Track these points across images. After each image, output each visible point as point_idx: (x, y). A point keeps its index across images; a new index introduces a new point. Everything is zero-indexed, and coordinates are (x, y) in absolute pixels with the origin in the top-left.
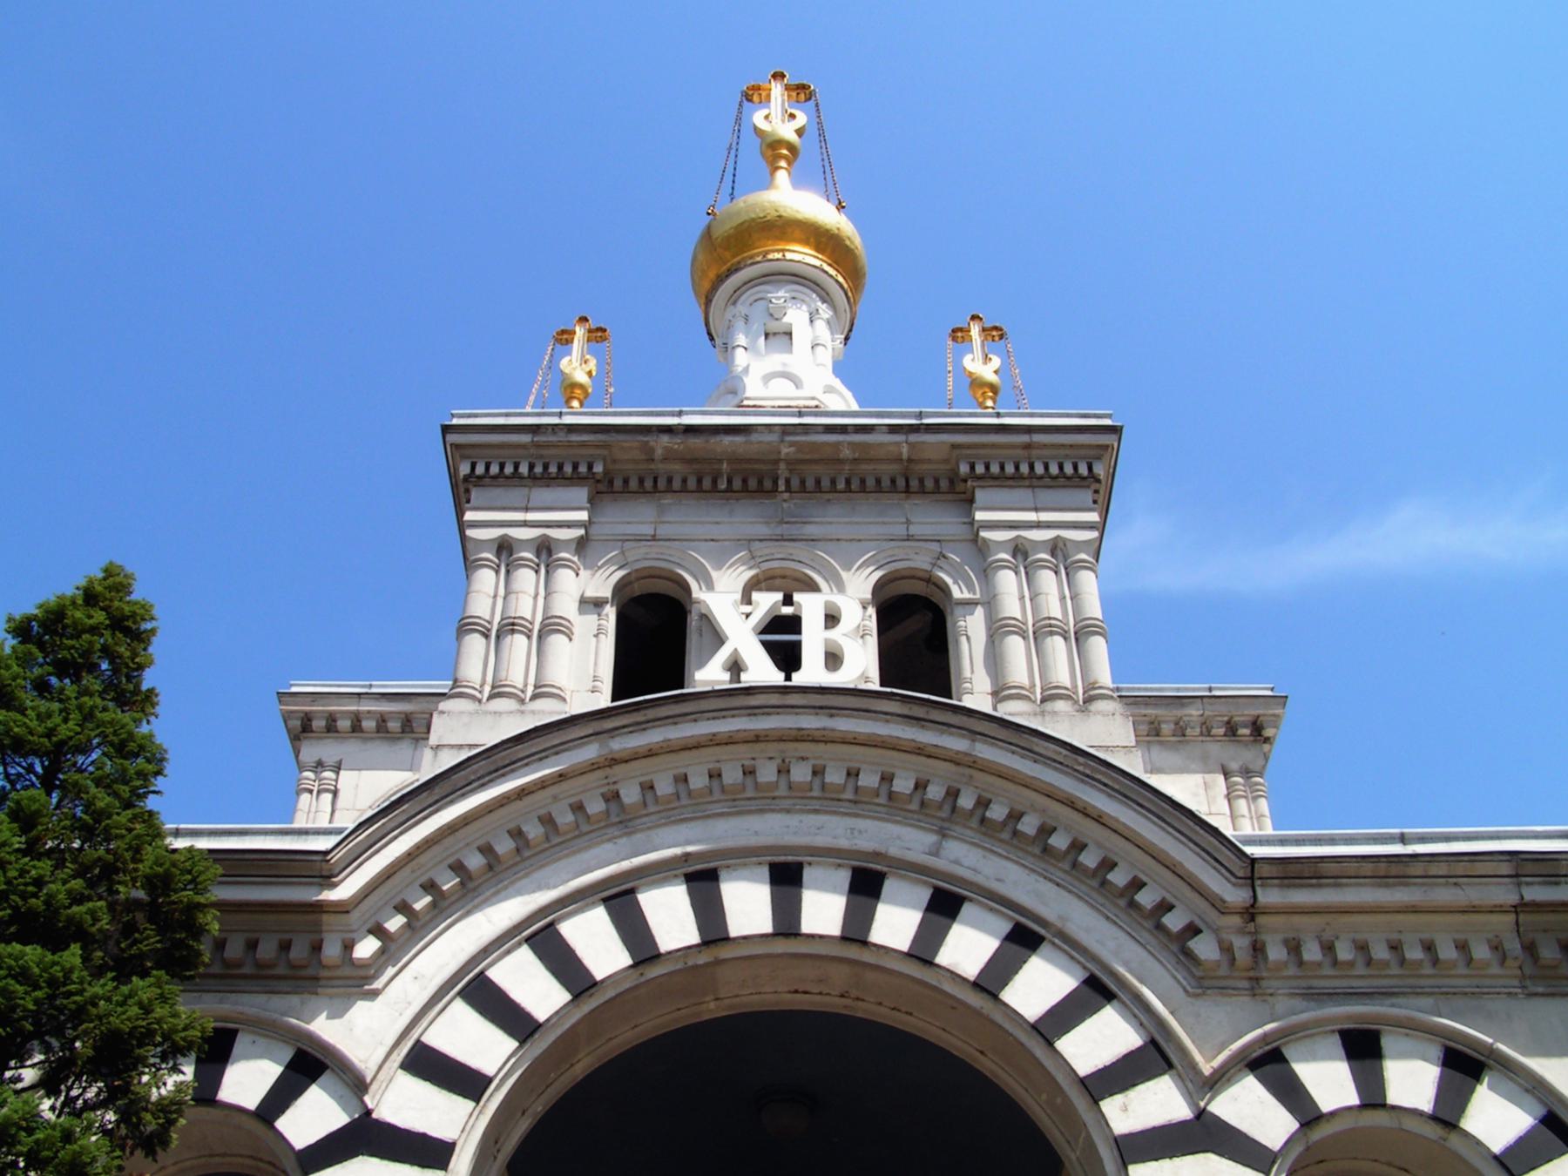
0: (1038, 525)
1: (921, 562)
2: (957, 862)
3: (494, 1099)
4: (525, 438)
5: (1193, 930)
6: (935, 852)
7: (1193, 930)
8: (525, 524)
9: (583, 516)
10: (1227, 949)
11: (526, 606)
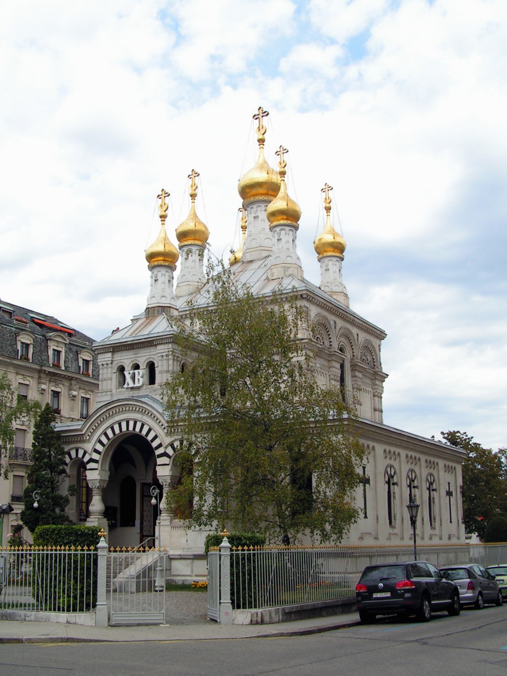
0: (164, 352)
1: (152, 360)
2: (143, 419)
3: (102, 454)
4: (101, 347)
6: (141, 418)
7: (164, 428)
8: (104, 361)
9: (110, 359)
10: (167, 430)
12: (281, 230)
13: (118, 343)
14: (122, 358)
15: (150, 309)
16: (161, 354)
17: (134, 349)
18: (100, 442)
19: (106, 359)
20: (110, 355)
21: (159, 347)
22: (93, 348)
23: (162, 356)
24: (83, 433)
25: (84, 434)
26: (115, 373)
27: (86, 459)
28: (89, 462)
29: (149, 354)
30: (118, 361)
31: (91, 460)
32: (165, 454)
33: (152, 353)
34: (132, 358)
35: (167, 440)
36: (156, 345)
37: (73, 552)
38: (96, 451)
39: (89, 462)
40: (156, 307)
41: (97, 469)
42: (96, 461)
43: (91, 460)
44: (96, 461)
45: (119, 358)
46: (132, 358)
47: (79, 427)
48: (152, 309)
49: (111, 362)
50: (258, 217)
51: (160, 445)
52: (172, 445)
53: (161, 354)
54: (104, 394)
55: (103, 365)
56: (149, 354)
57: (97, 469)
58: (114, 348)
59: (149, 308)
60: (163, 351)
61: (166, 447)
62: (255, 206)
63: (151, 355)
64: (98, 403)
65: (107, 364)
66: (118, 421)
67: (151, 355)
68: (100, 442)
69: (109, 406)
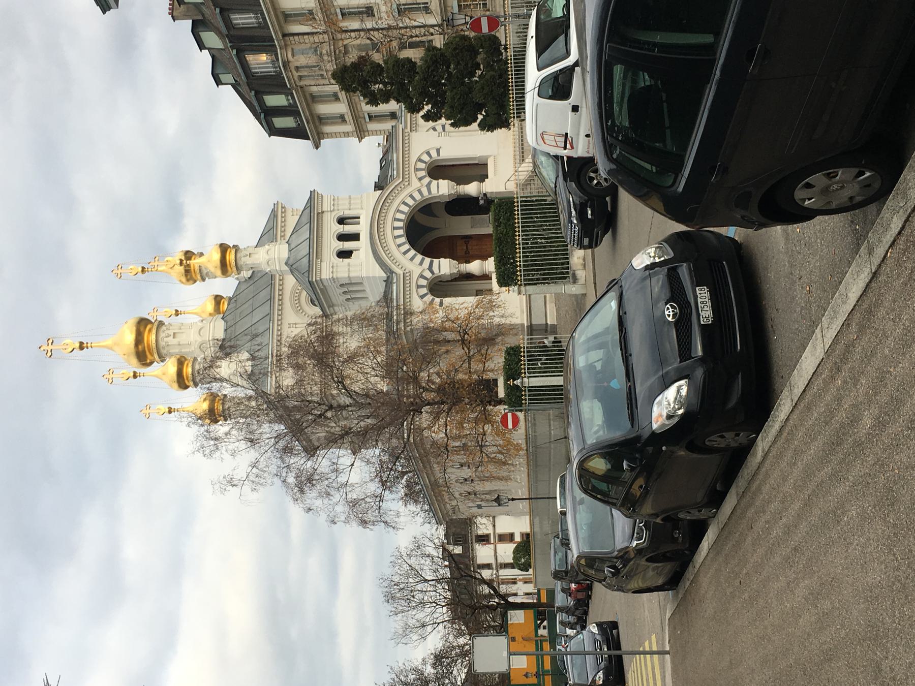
20: (324, 264)
25: (404, 274)
27: (428, 274)
28: (432, 272)
31: (430, 268)
35: (416, 184)
37: (526, 354)
39: (432, 272)
41: (439, 261)
42: (431, 264)
43: (430, 268)
44: (431, 264)
51: (420, 191)
52: (420, 179)
57: (439, 261)
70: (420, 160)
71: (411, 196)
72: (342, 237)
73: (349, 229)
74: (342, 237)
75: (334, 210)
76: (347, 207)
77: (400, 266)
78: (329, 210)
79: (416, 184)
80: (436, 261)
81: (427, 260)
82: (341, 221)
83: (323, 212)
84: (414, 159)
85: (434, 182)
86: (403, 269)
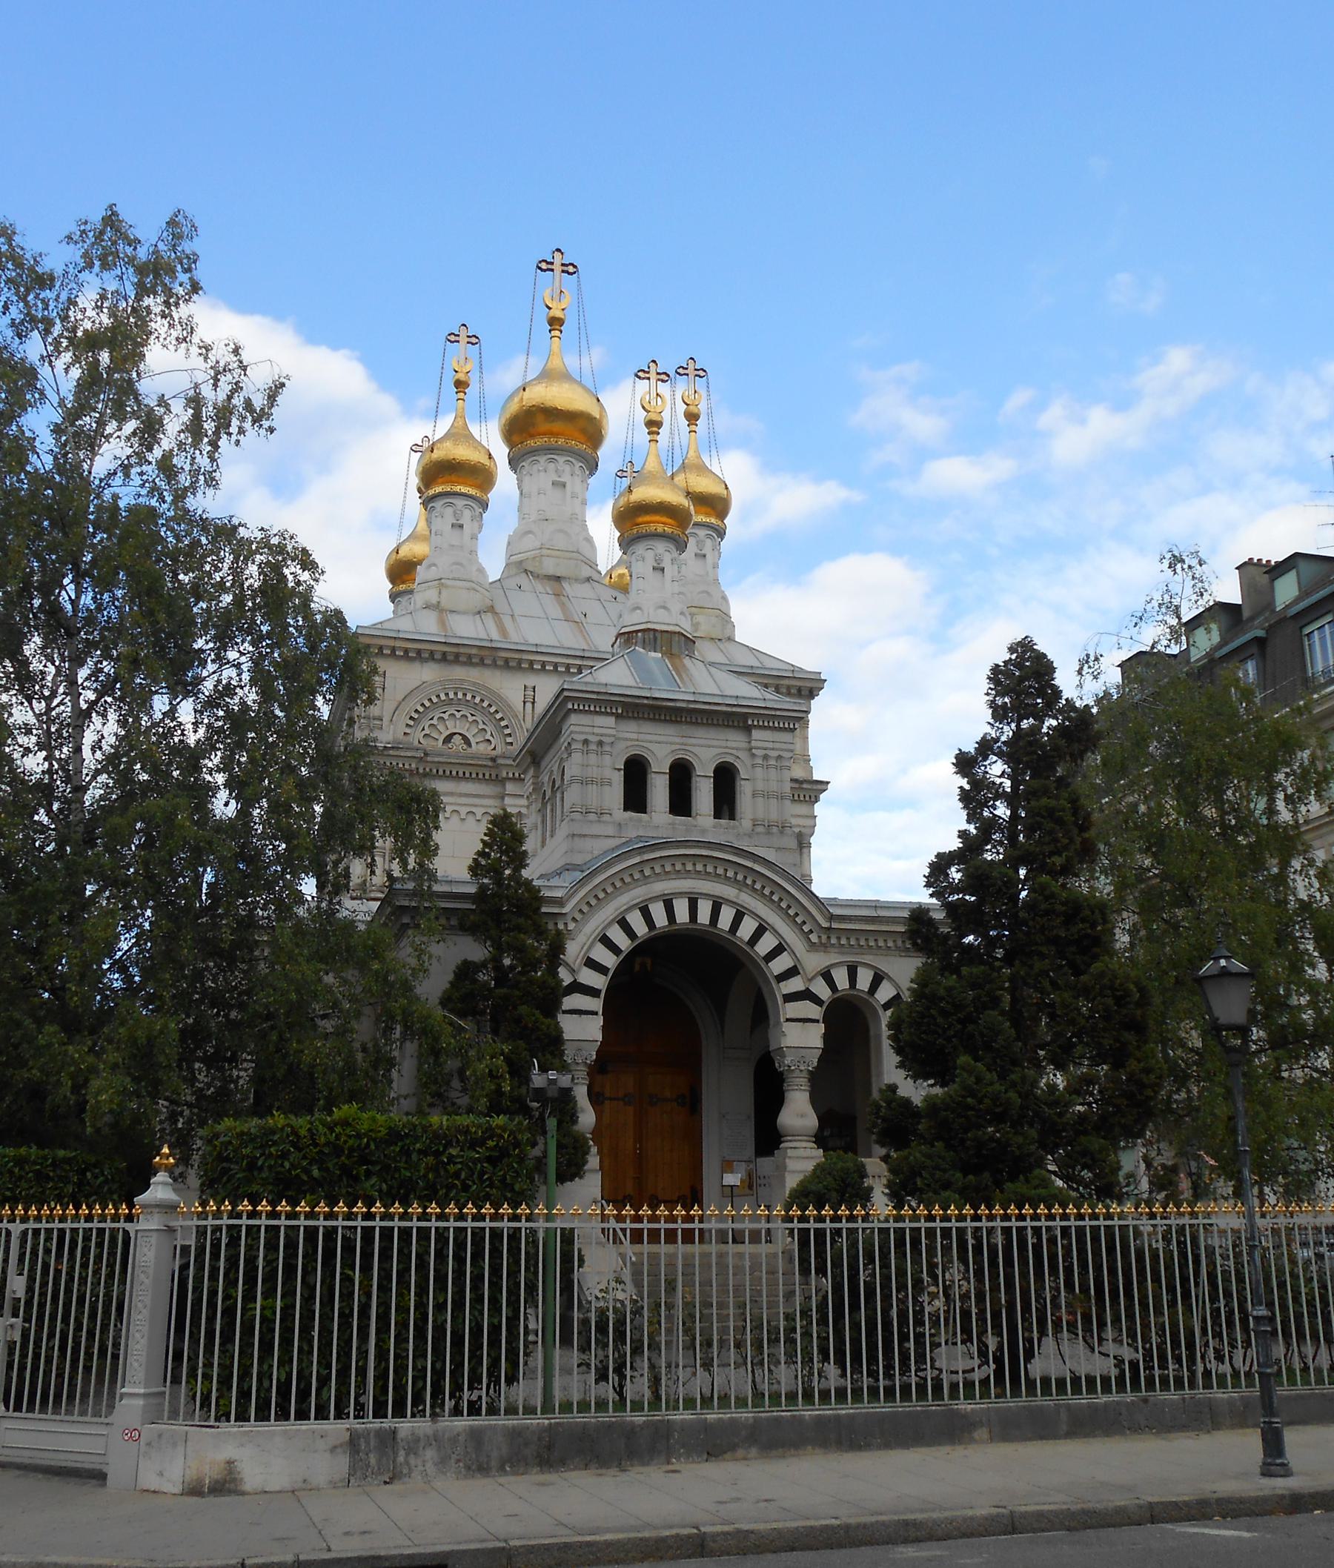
0: (773, 749)
5: (811, 931)
6: (737, 897)
7: (811, 931)
11: (593, 772)
12: (709, 536)
13: (647, 698)
14: (642, 737)
15: (658, 635)
16: (764, 752)
17: (681, 722)
18: (606, 941)
19: (596, 730)
20: (611, 721)
21: (756, 734)
22: (566, 694)
23: (766, 757)
24: (564, 911)
26: (619, 770)
29: (724, 744)
30: (630, 743)
31: (577, 987)
32: (807, 995)
33: (729, 744)
34: (671, 743)
35: (814, 962)
36: (748, 729)
38: (592, 964)
40: (675, 633)
41: (596, 1013)
42: (592, 992)
43: (577, 987)
44: (592, 992)
45: (634, 736)
46: (671, 743)
47: (558, 894)
48: (665, 634)
49: (612, 739)
50: (564, 485)
51: (792, 972)
53: (764, 752)
54: (592, 817)
55: (586, 742)
56: (724, 744)
57: (596, 1013)
58: (623, 704)
59: (655, 630)
60: (770, 745)
61: (810, 980)
62: (542, 459)
63: (727, 747)
64: (576, 838)
65: (600, 743)
66: (665, 895)
67: (727, 747)
68: (606, 941)
69: (653, 851)
70: (878, 979)
71: (778, 950)
72: (681, 775)
73: (703, 795)
74: (681, 775)
75: (753, 755)
76: (760, 786)
77: (585, 909)
78: (754, 744)
79: (814, 962)
80: (596, 1004)
81: (599, 981)
82: (725, 778)
83: (748, 729)
84: (885, 965)
85: (814, 1011)
86: (578, 916)
